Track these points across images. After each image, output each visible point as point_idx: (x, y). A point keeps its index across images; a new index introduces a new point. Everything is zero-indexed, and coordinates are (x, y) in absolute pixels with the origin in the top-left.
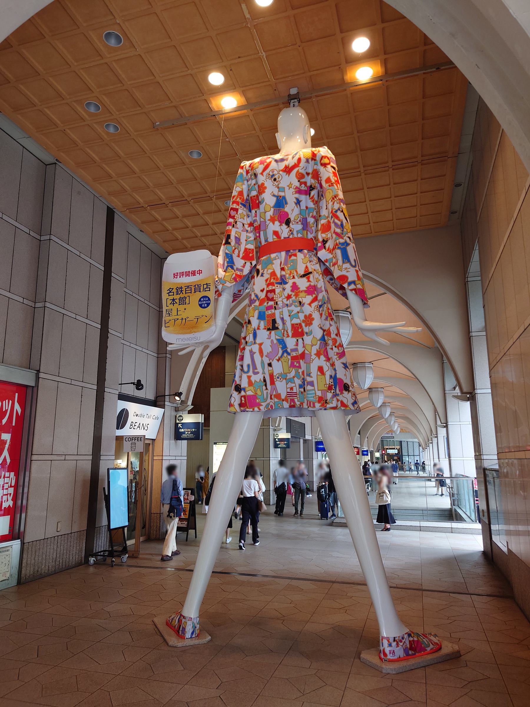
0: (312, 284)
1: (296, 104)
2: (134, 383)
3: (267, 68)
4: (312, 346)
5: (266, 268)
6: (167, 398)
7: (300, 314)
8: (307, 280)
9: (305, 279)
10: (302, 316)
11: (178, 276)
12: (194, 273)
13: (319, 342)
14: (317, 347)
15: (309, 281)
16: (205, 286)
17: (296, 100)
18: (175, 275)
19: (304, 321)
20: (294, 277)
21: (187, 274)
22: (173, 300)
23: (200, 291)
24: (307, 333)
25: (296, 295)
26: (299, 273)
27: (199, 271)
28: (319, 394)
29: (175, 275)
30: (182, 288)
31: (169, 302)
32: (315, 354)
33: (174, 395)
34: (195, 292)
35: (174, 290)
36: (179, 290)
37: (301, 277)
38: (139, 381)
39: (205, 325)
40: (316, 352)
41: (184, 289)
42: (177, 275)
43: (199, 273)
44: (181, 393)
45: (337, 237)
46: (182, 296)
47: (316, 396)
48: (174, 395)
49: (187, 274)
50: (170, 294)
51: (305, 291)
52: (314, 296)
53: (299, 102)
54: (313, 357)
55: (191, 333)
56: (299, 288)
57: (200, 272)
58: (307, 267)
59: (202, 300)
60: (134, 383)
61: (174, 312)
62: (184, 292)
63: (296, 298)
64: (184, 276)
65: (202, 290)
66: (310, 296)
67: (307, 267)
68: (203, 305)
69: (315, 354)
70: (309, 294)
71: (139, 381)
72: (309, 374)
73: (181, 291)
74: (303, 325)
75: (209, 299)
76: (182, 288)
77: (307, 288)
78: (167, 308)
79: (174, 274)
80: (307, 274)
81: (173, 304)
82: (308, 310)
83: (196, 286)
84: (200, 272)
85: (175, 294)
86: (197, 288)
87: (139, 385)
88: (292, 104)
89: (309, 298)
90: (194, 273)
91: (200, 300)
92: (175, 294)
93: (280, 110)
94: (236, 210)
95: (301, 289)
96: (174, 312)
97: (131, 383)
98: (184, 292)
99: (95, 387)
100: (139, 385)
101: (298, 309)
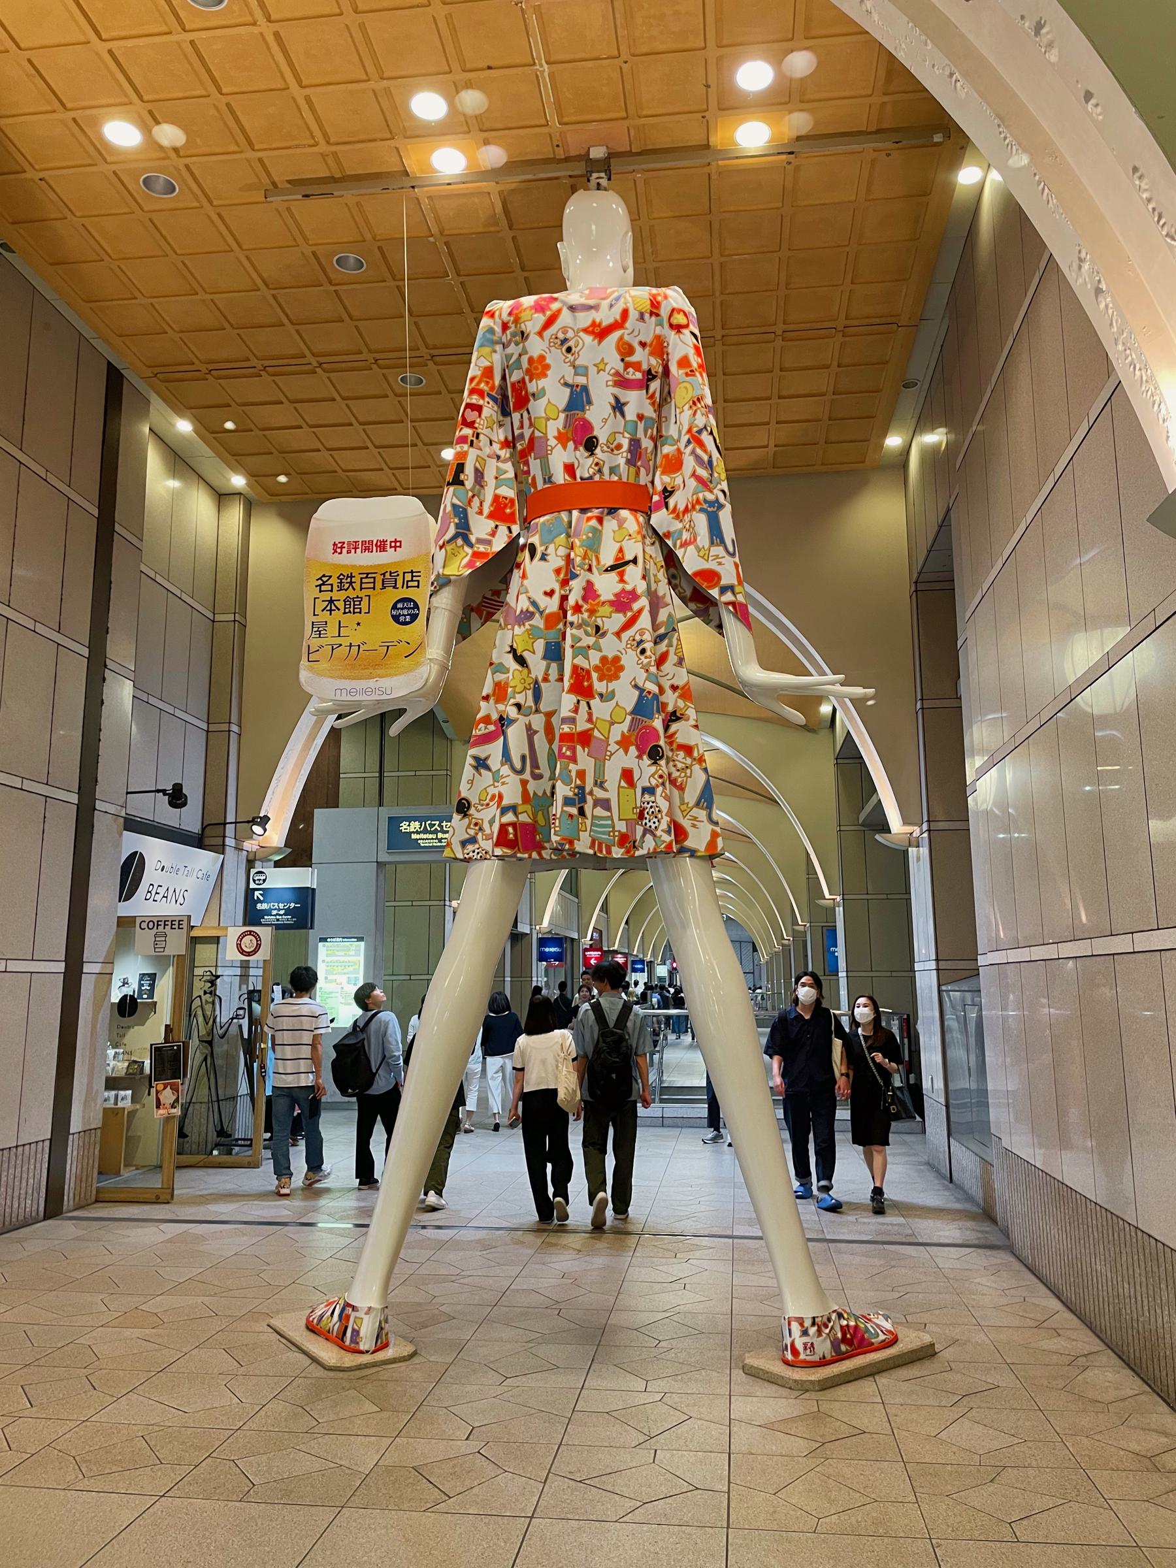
0: (629, 588)
1: (604, 182)
2: (164, 792)
3: (549, 97)
4: (612, 723)
5: (552, 541)
6: (230, 829)
7: (591, 652)
8: (617, 579)
9: (613, 576)
10: (595, 658)
11: (345, 551)
12: (382, 546)
13: (629, 718)
14: (625, 727)
15: (622, 581)
16: (408, 577)
17: (603, 175)
18: (337, 548)
19: (596, 668)
20: (590, 570)
21: (367, 547)
22: (331, 601)
23: (395, 587)
24: (601, 695)
25: (592, 612)
26: (602, 563)
27: (396, 541)
28: (621, 827)
29: (337, 548)
30: (352, 577)
31: (321, 605)
32: (617, 743)
33: (248, 822)
34: (384, 588)
35: (334, 581)
36: (347, 580)
37: (606, 570)
38: (178, 788)
39: (405, 662)
40: (619, 738)
41: (357, 579)
42: (342, 548)
43: (395, 547)
44: (265, 820)
45: (701, 487)
46: (351, 593)
47: (614, 831)
48: (248, 822)
49: (367, 547)
50: (323, 588)
51: (612, 603)
52: (629, 614)
53: (609, 179)
54: (613, 747)
55: (370, 677)
56: (599, 596)
57: (396, 545)
58: (621, 550)
59: (400, 605)
60: (164, 792)
61: (332, 630)
62: (357, 586)
63: (590, 617)
64: (359, 551)
65: (399, 584)
66: (620, 615)
67: (621, 550)
68: (402, 619)
69: (617, 743)
70: (618, 611)
71: (178, 788)
72: (602, 783)
73: (351, 583)
74: (595, 675)
75: (416, 606)
76: (352, 577)
77: (616, 595)
78: (315, 619)
79: (335, 544)
80: (619, 566)
81: (331, 610)
82: (610, 646)
83: (387, 576)
84: (396, 545)
85: (335, 588)
86: (389, 579)
87: (177, 797)
88: (593, 183)
89: (620, 619)
90: (382, 546)
91: (394, 607)
92: (335, 588)
93: (574, 190)
94: (478, 409)
95: (602, 599)
96: (332, 630)
97: (158, 791)
98: (357, 586)
99: (74, 798)
100: (177, 797)
101: (591, 641)
